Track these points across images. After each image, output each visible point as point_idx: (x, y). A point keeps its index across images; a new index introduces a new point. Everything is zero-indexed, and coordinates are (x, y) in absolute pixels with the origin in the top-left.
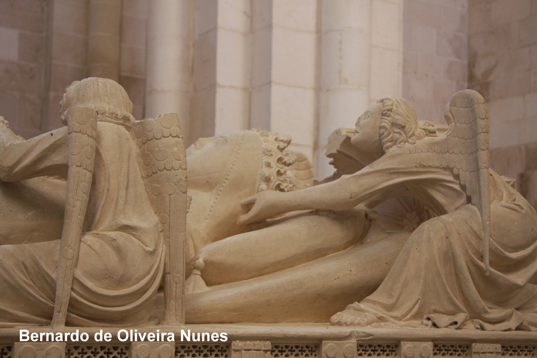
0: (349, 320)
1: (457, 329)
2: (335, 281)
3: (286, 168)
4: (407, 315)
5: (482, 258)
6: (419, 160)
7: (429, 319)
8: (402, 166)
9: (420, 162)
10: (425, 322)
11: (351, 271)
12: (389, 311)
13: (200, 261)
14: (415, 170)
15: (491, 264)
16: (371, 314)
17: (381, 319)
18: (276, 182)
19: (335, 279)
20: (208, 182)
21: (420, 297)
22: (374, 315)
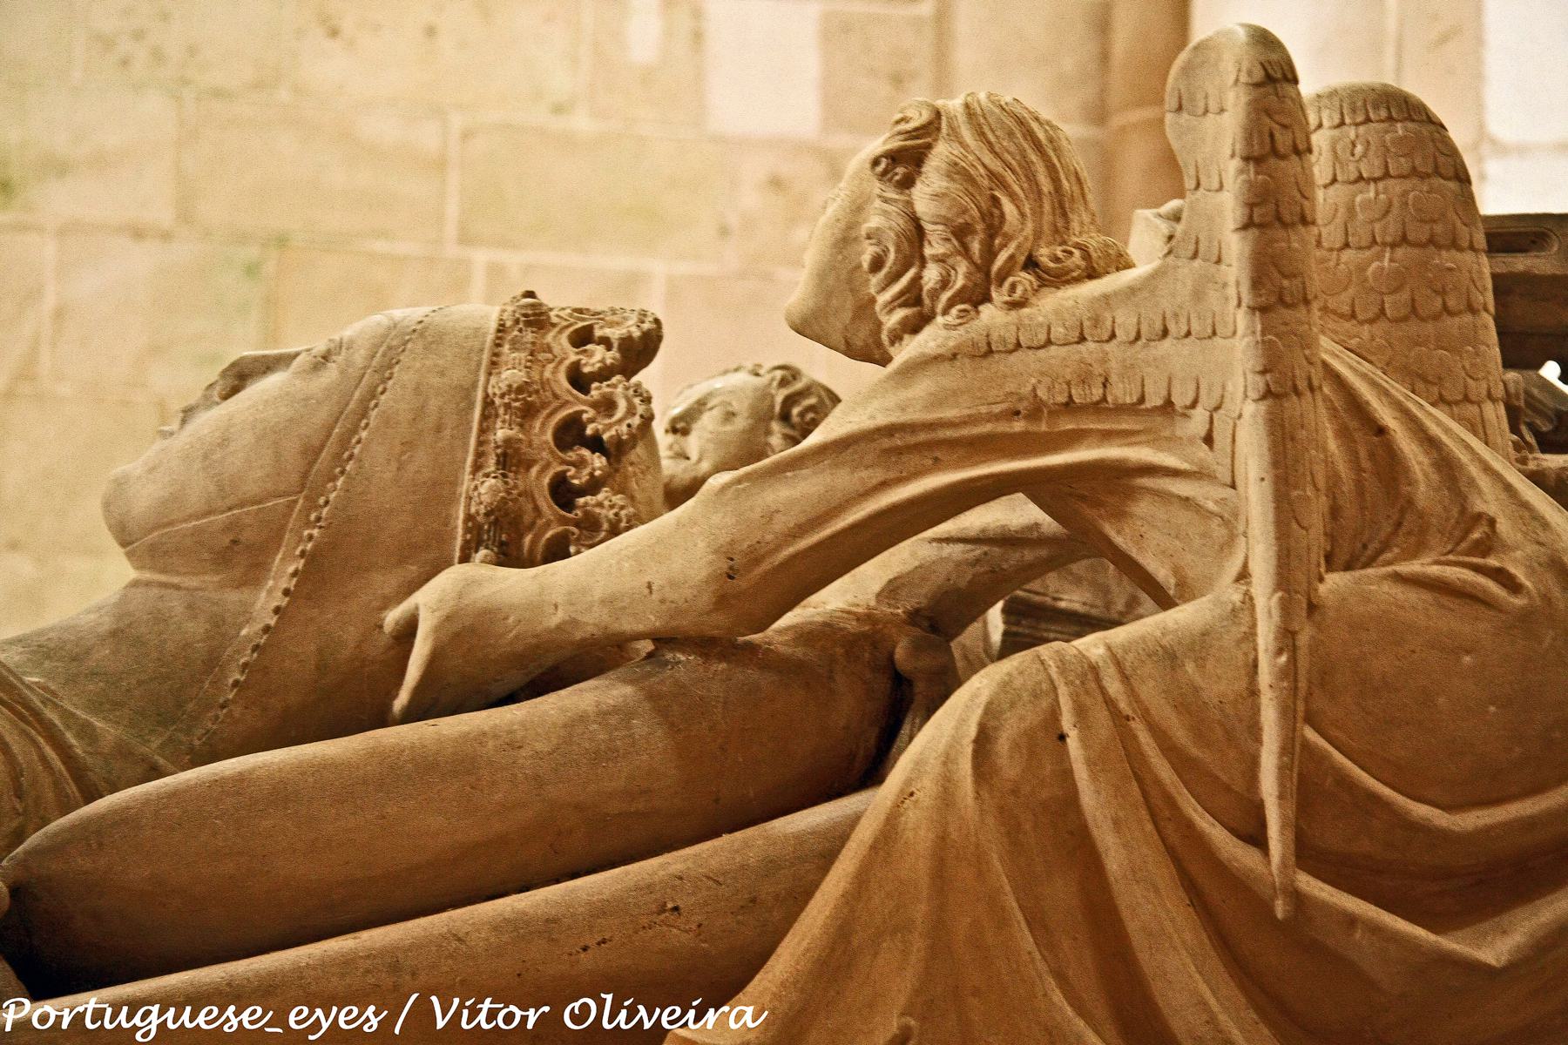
3: (598, 462)
5: (1257, 839)
6: (1033, 381)
8: (949, 413)
9: (1034, 389)
11: (676, 909)
14: (1018, 426)
20: (234, 542)
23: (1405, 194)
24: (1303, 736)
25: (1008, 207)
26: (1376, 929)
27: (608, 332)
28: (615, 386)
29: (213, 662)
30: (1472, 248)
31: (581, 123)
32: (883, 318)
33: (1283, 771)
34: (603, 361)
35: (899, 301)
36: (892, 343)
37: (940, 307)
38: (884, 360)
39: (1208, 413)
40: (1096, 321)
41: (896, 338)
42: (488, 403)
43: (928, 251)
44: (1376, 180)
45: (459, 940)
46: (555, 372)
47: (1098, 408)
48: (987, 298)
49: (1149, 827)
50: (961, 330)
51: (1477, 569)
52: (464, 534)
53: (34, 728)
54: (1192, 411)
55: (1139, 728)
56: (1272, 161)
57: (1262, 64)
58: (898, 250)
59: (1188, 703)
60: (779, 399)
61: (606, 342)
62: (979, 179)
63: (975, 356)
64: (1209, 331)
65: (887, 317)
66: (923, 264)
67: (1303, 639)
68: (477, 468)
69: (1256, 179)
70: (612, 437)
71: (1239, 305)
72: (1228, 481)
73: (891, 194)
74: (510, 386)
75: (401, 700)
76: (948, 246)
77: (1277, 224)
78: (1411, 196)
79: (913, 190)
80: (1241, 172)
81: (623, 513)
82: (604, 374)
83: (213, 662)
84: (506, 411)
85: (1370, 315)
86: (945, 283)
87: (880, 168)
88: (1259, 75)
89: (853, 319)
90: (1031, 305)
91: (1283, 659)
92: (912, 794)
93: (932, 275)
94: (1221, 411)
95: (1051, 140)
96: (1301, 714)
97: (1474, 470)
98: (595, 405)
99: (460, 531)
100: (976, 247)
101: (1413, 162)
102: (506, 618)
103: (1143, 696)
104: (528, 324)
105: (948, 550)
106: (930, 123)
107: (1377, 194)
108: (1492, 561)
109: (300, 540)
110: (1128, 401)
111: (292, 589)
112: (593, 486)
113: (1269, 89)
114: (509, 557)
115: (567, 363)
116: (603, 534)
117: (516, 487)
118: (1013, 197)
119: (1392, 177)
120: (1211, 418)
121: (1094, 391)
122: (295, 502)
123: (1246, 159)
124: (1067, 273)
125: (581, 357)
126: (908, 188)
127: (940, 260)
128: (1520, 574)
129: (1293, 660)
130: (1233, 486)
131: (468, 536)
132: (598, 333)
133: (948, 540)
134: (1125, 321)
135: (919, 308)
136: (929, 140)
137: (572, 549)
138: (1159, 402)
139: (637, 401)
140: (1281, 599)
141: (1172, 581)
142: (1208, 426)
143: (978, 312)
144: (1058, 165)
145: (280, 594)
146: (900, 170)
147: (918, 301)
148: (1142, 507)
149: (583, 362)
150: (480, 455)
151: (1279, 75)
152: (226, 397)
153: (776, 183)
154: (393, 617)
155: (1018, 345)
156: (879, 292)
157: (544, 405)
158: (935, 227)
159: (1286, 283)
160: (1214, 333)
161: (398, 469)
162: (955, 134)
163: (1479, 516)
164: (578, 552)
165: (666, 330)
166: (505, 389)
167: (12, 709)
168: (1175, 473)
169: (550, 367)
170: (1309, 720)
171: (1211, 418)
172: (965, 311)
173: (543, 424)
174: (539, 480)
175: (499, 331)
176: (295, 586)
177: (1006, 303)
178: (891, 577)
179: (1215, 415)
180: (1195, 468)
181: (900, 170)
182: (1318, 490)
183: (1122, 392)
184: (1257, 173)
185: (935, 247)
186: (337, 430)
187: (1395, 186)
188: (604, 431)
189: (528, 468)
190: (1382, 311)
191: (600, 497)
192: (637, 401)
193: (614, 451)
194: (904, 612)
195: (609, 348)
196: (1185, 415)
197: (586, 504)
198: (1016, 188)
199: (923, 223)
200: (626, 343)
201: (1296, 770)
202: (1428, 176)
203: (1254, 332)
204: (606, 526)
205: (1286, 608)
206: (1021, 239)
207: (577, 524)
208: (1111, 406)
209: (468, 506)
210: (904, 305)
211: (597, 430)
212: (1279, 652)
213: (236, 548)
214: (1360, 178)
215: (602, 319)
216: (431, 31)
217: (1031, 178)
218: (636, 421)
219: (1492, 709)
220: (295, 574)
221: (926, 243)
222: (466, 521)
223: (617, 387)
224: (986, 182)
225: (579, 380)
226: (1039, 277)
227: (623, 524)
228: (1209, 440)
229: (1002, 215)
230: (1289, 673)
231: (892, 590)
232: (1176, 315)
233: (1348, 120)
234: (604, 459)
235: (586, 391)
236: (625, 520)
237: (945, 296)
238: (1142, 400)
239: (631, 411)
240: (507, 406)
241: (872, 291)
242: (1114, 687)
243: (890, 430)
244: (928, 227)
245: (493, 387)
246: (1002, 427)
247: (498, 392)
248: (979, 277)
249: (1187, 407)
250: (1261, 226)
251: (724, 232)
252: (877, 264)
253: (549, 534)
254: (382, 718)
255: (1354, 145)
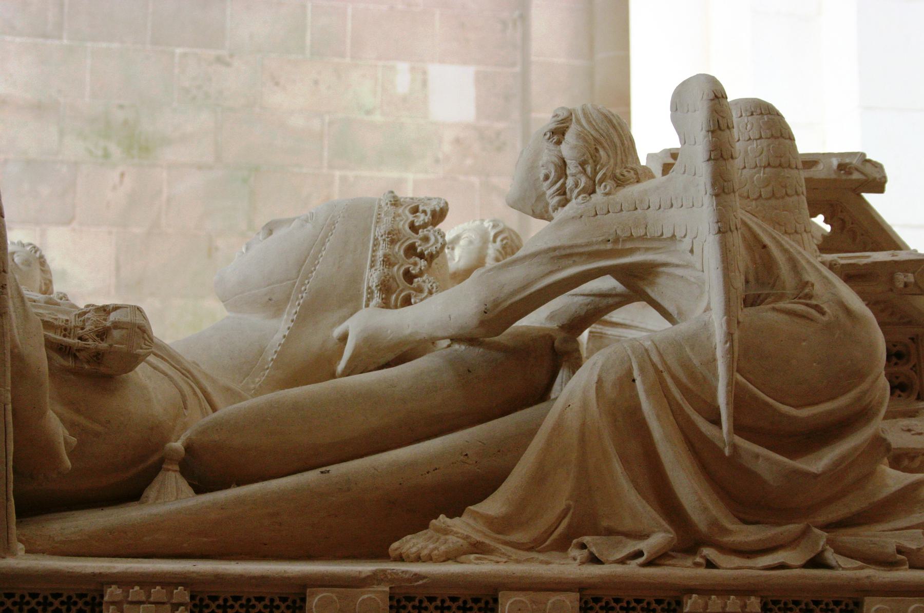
0: (414, 550)
1: (644, 565)
2: (427, 475)
3: (423, 263)
4: (545, 541)
6: (615, 227)
7: (583, 546)
8: (579, 241)
9: (616, 231)
10: (574, 552)
11: (466, 455)
12: (499, 533)
13: (177, 445)
14: (609, 246)
15: (739, 428)
16: (457, 537)
17: (478, 549)
18: (402, 291)
19: (428, 473)
20: (270, 300)
21: (571, 503)
22: (464, 539)
23: (769, 145)
24: (736, 378)
25: (602, 152)
26: (767, 459)
27: (425, 208)
28: (429, 231)
29: (262, 351)
30: (796, 168)
31: (377, 118)
32: (549, 201)
33: (728, 393)
34: (424, 220)
35: (556, 194)
36: (554, 211)
37: (574, 196)
38: (550, 219)
39: (691, 240)
40: (641, 202)
41: (555, 209)
42: (376, 239)
43: (568, 172)
44: (756, 140)
45: (375, 469)
46: (404, 224)
47: (643, 238)
48: (594, 192)
49: (672, 418)
50: (583, 205)
51: (807, 305)
52: (367, 295)
53: (190, 379)
54: (684, 240)
55: (665, 374)
56: (719, 132)
57: (713, 91)
58: (556, 171)
59: (686, 365)
60: (492, 234)
61: (424, 212)
62: (589, 141)
63: (589, 216)
64: (691, 204)
65: (551, 201)
66: (566, 178)
67: (736, 336)
68: (372, 267)
69: (712, 140)
70: (429, 253)
71: (706, 193)
72: (701, 269)
73: (552, 147)
74: (385, 232)
75: (341, 366)
76: (577, 169)
77: (721, 159)
78: (771, 146)
79: (561, 146)
80: (705, 137)
81: (434, 285)
82: (425, 226)
83: (262, 351)
84: (384, 241)
85: (755, 197)
86: (577, 185)
87: (548, 136)
88: (712, 96)
89: (536, 201)
90: (613, 194)
91: (728, 345)
92: (569, 406)
93: (570, 182)
94: (697, 239)
95: (619, 124)
96: (735, 369)
97: (803, 263)
98: (421, 239)
99: (365, 294)
100: (589, 169)
101: (772, 132)
102: (387, 331)
103: (668, 362)
104: (392, 205)
105: (576, 299)
106: (568, 117)
107: (757, 146)
108: (814, 302)
109: (297, 299)
110: (656, 235)
111: (295, 319)
112: (421, 274)
113: (717, 101)
114: (386, 304)
115: (409, 221)
116: (425, 294)
117: (388, 274)
118: (604, 148)
119: (763, 138)
120: (693, 242)
121: (641, 230)
122: (295, 282)
123: (708, 131)
124: (630, 179)
125: (414, 219)
126: (559, 145)
127: (573, 175)
128: (826, 308)
129: (732, 346)
130: (703, 271)
131: (369, 296)
132: (421, 208)
133: (576, 295)
134: (654, 200)
135: (564, 196)
136: (568, 124)
137: (413, 301)
138: (670, 235)
139: (439, 237)
140: (727, 318)
141: (676, 312)
142: (691, 246)
143: (591, 198)
144: (623, 134)
145: (290, 321)
146: (556, 138)
147: (564, 193)
148: (662, 280)
149: (415, 221)
150: (373, 261)
151: (720, 96)
152: (265, 239)
153: (457, 141)
154: (337, 332)
155: (609, 212)
156: (548, 190)
157: (399, 240)
158: (571, 162)
159: (726, 184)
160: (693, 206)
161: (338, 268)
162: (578, 121)
163: (807, 283)
164: (415, 303)
165: (450, 206)
166: (383, 233)
167: (181, 372)
168: (677, 266)
169: (402, 223)
170: (738, 371)
171: (693, 242)
172: (585, 197)
173: (400, 248)
174: (397, 271)
175: (379, 208)
176: (296, 318)
177: (602, 193)
178: (551, 311)
179: (694, 241)
180: (685, 264)
181: (556, 138)
182: (740, 272)
183: (653, 231)
184: (712, 137)
185: (572, 169)
186: (312, 251)
187: (764, 142)
188: (425, 251)
189: (394, 266)
190: (760, 196)
191: (424, 278)
192: (439, 237)
193: (431, 258)
194: (557, 326)
195: (426, 215)
196: (680, 241)
197: (418, 281)
198: (606, 145)
199: (565, 159)
200: (434, 213)
201: (733, 392)
202: (778, 138)
203: (713, 205)
204: (426, 291)
205: (729, 323)
206: (608, 166)
207: (414, 289)
208: (649, 237)
209: (368, 283)
210: (559, 195)
211: (422, 250)
212: (726, 342)
213: (270, 302)
214: (750, 139)
215: (423, 202)
216: (316, 83)
217: (612, 141)
218: (439, 245)
219: (814, 364)
220: (296, 313)
221: (567, 168)
222: (367, 290)
223: (430, 232)
224: (593, 142)
225: (414, 228)
226: (616, 182)
227: (434, 290)
228: (692, 251)
229: (600, 155)
230: (730, 351)
231: (551, 317)
232: (676, 198)
233: (744, 115)
234: (426, 262)
235: (417, 233)
236: (435, 288)
237: (576, 191)
238: (662, 234)
239: (437, 241)
240: (384, 240)
241: (545, 189)
242: (656, 358)
243: (554, 249)
244: (568, 162)
245: (378, 232)
246: (602, 247)
247: (380, 234)
248: (591, 182)
249: (682, 237)
250: (714, 160)
251: (437, 161)
252: (547, 178)
253: (403, 294)
254: (333, 376)
255: (747, 126)
